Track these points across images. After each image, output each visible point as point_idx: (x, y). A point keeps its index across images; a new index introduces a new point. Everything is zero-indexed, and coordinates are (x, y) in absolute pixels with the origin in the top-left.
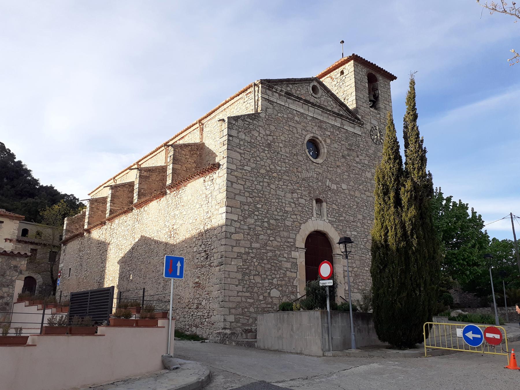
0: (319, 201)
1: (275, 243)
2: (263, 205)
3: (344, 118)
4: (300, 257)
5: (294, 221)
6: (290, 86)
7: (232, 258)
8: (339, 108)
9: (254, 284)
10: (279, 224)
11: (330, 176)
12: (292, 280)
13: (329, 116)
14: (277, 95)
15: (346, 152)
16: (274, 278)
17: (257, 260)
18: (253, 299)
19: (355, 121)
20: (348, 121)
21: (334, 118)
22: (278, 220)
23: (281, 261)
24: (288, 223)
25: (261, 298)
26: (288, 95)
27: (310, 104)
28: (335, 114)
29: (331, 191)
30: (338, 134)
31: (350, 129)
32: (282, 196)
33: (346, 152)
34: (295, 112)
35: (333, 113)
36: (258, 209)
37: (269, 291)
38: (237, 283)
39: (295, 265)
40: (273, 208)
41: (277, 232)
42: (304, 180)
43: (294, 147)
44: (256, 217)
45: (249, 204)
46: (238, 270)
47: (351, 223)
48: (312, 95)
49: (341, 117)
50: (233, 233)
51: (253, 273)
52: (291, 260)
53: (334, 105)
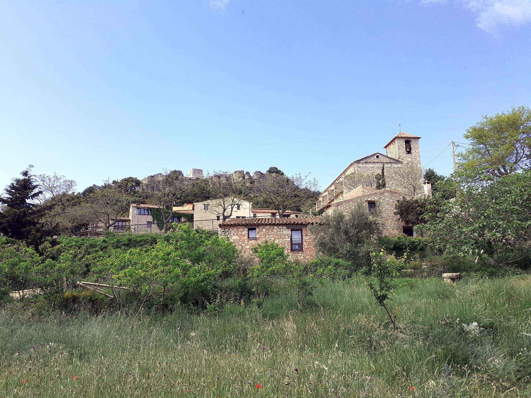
14: (362, 164)
15: (394, 175)
31: (395, 166)
33: (394, 175)
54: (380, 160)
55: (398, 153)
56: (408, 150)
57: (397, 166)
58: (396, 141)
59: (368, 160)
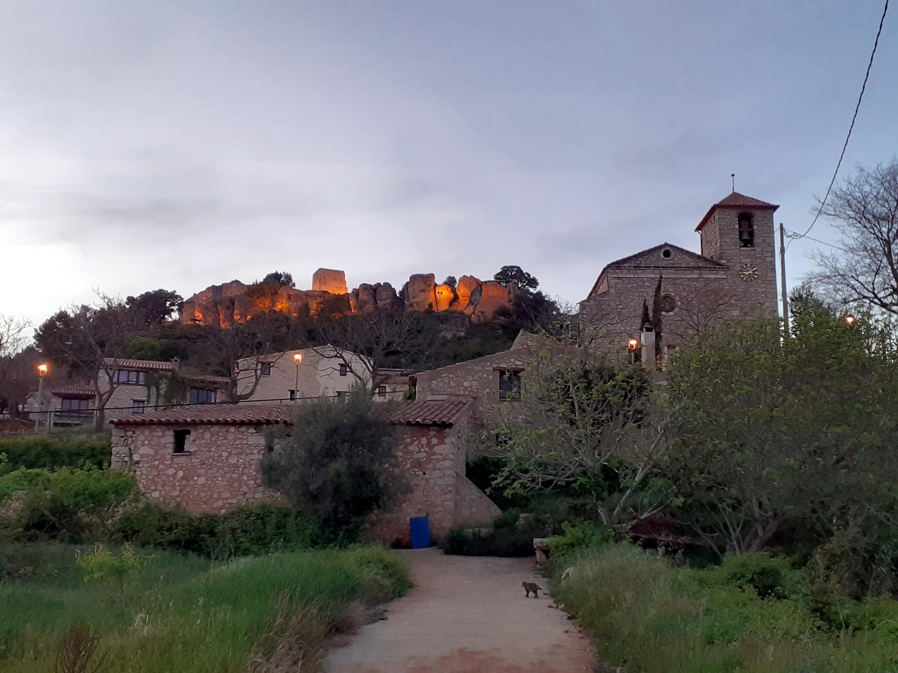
6: (640, 259)
8: (697, 260)
13: (685, 272)
21: (690, 272)
31: (710, 276)
48: (663, 259)
53: (691, 260)
54: (671, 262)
55: (718, 244)
56: (746, 237)
57: (714, 276)
58: (716, 214)
59: (643, 262)
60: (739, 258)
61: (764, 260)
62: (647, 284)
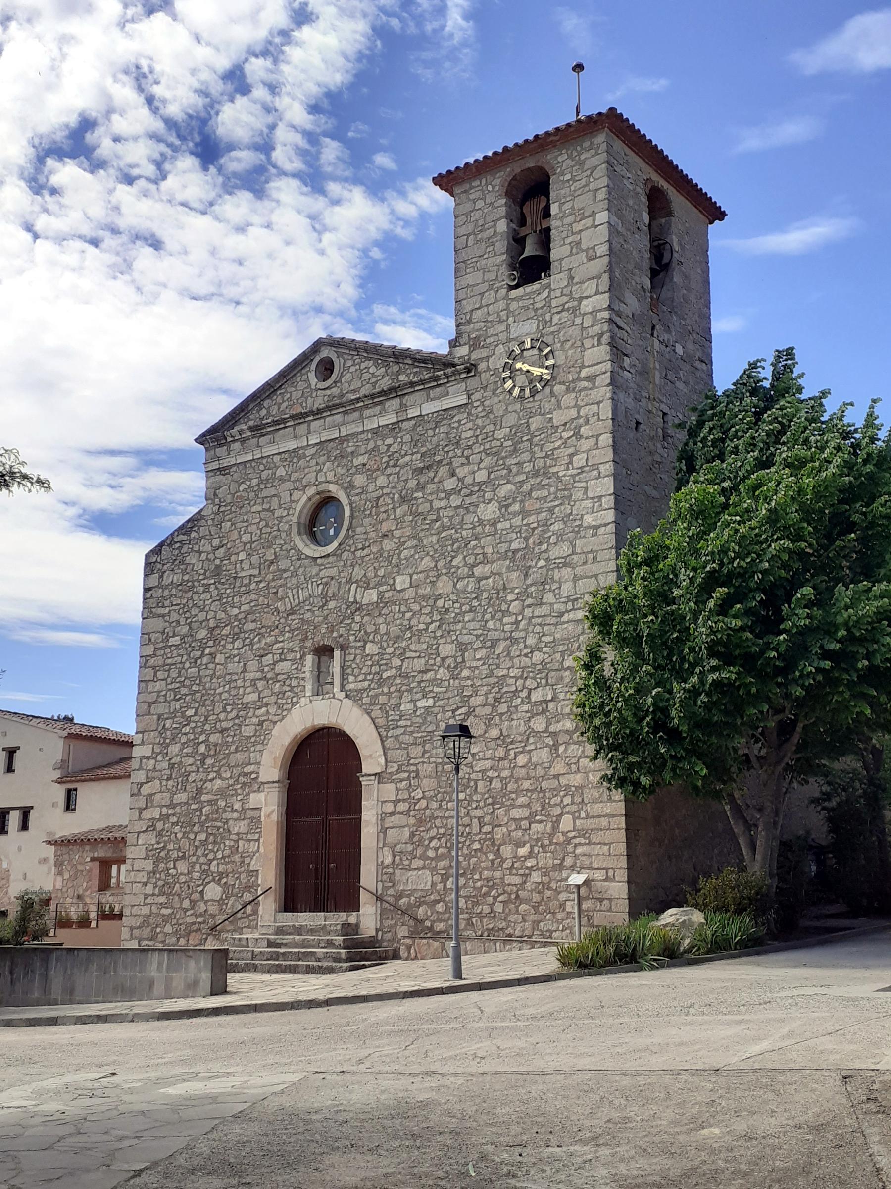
0: (324, 652)
1: (218, 783)
2: (198, 708)
3: (406, 391)
4: (266, 805)
5: (261, 723)
7: (139, 833)
8: (396, 368)
9: (173, 876)
10: (230, 739)
11: (358, 572)
12: (247, 860)
13: (367, 412)
16: (211, 861)
17: (181, 827)
18: (172, 907)
19: (438, 376)
20: (422, 387)
21: (378, 408)
22: (227, 729)
23: (227, 821)
24: (248, 731)
25: (186, 904)
26: (258, 430)
27: (308, 416)
28: (379, 397)
29: (363, 610)
30: (389, 446)
32: (237, 674)
33: (412, 484)
34: (277, 459)
35: (373, 399)
36: (188, 720)
37: (201, 888)
38: (145, 880)
39: (255, 822)
40: (219, 707)
41: (224, 758)
42: (292, 612)
43: (270, 544)
44: (184, 739)
45: (173, 715)
46: (147, 855)
47: (415, 676)
49: (396, 392)
50: (142, 784)
51: (175, 854)
52: (250, 814)
54: (335, 391)
60: (503, 327)
61: (574, 311)
62: (281, 472)
